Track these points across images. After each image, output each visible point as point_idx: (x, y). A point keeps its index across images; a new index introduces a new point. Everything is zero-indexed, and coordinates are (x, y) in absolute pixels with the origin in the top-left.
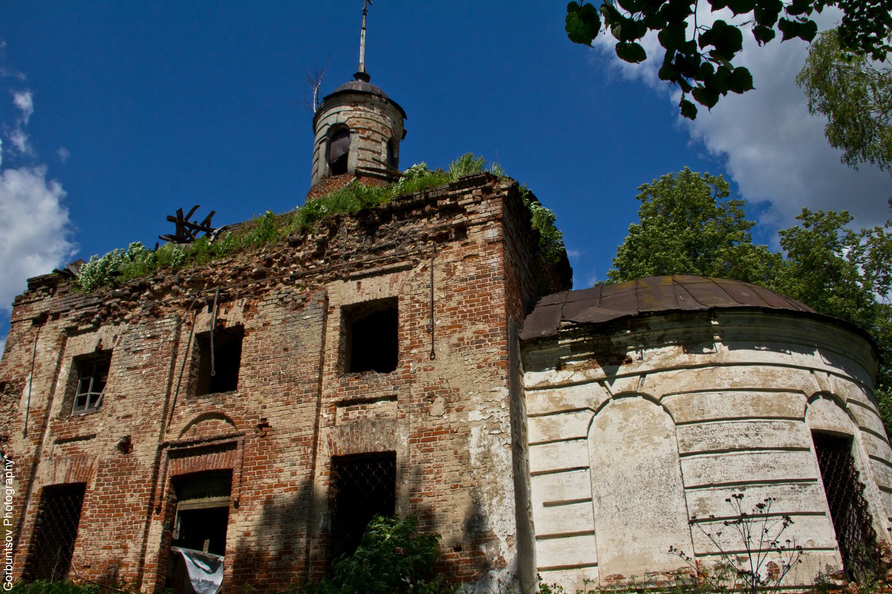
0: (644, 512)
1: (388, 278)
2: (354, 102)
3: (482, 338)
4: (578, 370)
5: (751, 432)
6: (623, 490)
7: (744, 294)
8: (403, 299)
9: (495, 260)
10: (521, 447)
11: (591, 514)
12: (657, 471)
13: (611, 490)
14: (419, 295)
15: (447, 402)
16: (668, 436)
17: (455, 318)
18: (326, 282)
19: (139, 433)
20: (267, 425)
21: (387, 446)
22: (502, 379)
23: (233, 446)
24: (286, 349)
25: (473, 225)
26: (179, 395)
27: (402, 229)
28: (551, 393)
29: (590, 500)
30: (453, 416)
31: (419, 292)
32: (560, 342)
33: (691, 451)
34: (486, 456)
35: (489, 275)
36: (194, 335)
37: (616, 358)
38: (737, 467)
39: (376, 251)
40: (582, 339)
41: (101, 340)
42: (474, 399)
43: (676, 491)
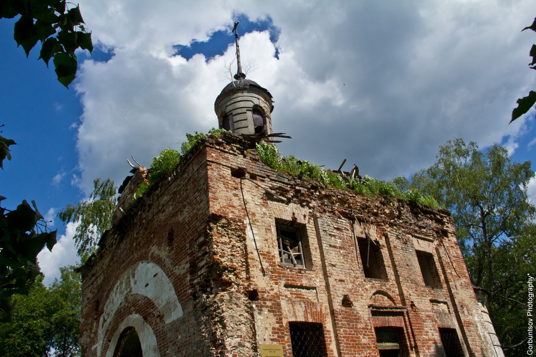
19: (353, 294)
30: (470, 317)
39: (420, 227)
41: (294, 214)
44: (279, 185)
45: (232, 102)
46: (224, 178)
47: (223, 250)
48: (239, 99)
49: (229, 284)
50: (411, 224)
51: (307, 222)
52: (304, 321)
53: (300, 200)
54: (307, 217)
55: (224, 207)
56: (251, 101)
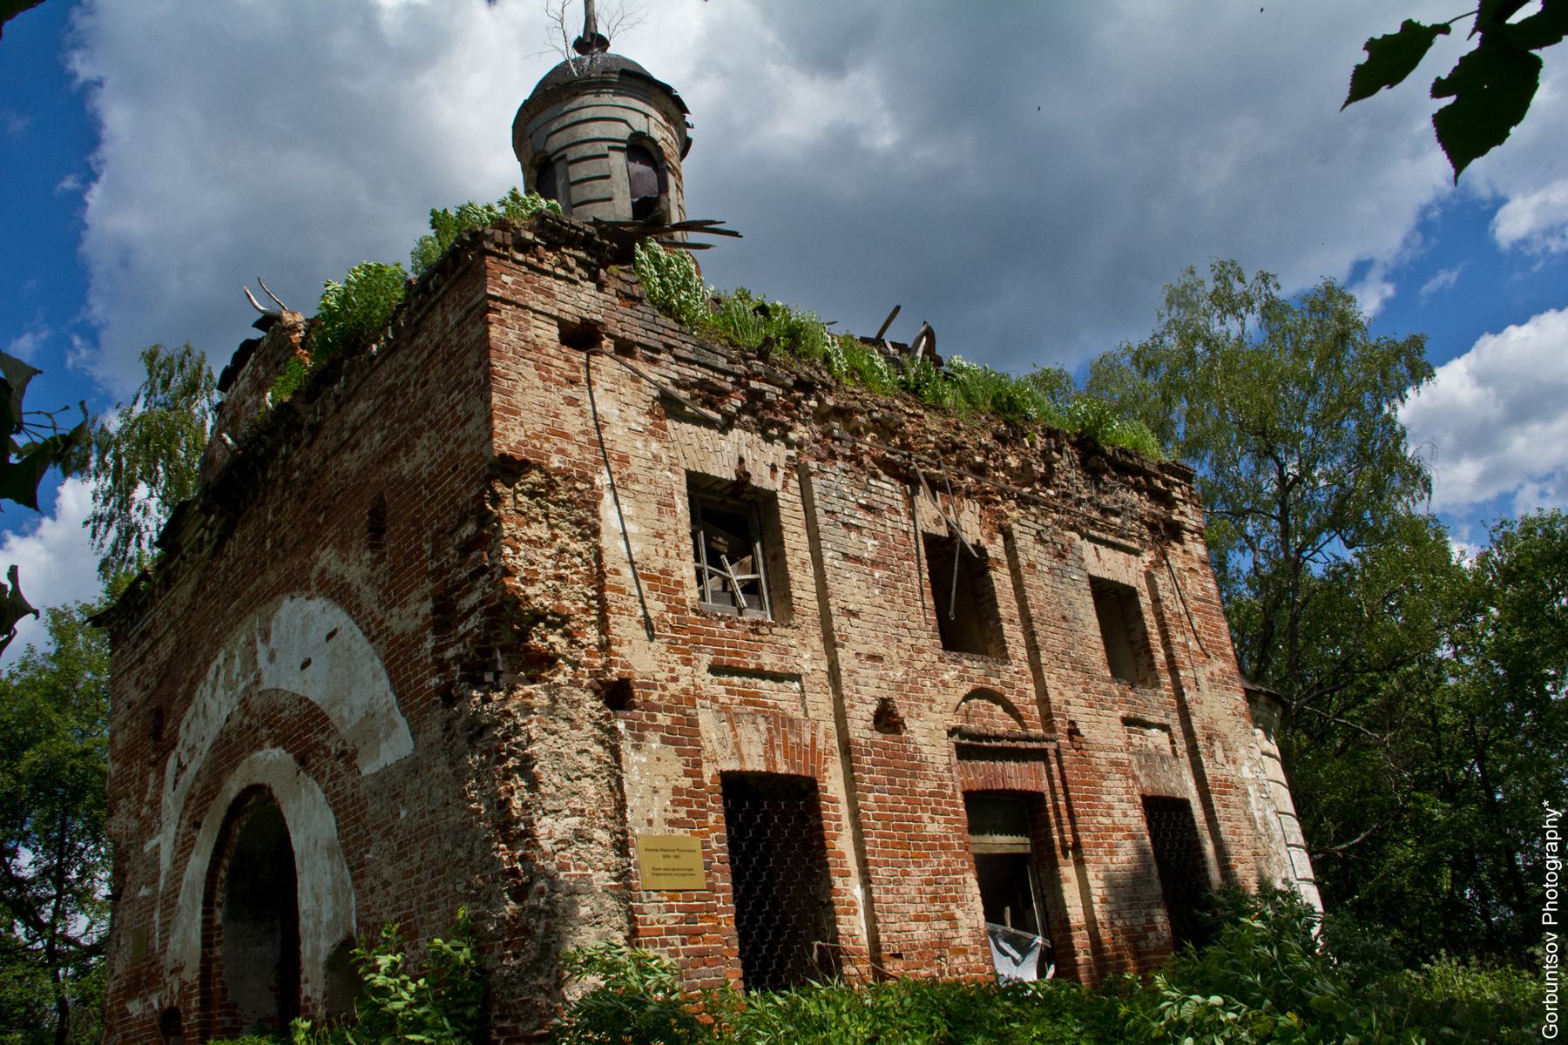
19: (907, 697)
30: (1231, 768)
39: (1105, 511)
41: (741, 460)
44: (700, 375)
45: (568, 120)
46: (538, 349)
47: (532, 564)
48: (587, 113)
49: (548, 661)
50: (1079, 502)
51: (779, 486)
52: (764, 769)
53: (761, 420)
54: (781, 472)
55: (537, 437)
56: (625, 121)
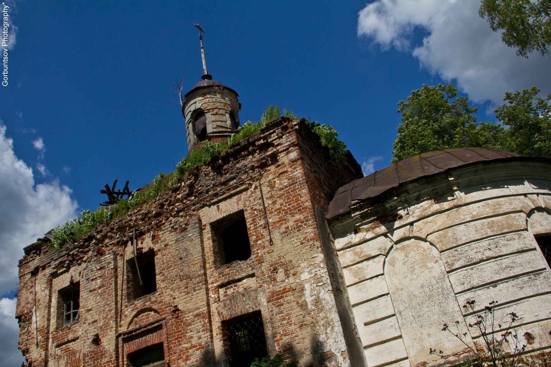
0: (431, 316)
1: (235, 199)
2: (204, 94)
3: (300, 224)
4: (369, 230)
5: (492, 246)
6: (414, 304)
7: (468, 155)
8: (246, 210)
9: (299, 171)
10: (340, 290)
11: (397, 325)
12: (434, 287)
13: (407, 305)
14: (256, 205)
15: (286, 271)
16: (437, 261)
17: (281, 215)
18: (198, 210)
19: (103, 331)
20: (178, 310)
21: (254, 307)
22: (318, 248)
23: (160, 327)
24: (181, 259)
25: (280, 152)
26: (123, 302)
27: (237, 166)
28: (355, 249)
29: (394, 315)
30: (291, 279)
31: (255, 203)
32: (353, 215)
33: (454, 268)
34: (317, 301)
35: (297, 182)
36: (125, 261)
37: (391, 217)
38: (488, 272)
40: (367, 210)
41: (72, 277)
42: (303, 265)
43: (450, 297)
